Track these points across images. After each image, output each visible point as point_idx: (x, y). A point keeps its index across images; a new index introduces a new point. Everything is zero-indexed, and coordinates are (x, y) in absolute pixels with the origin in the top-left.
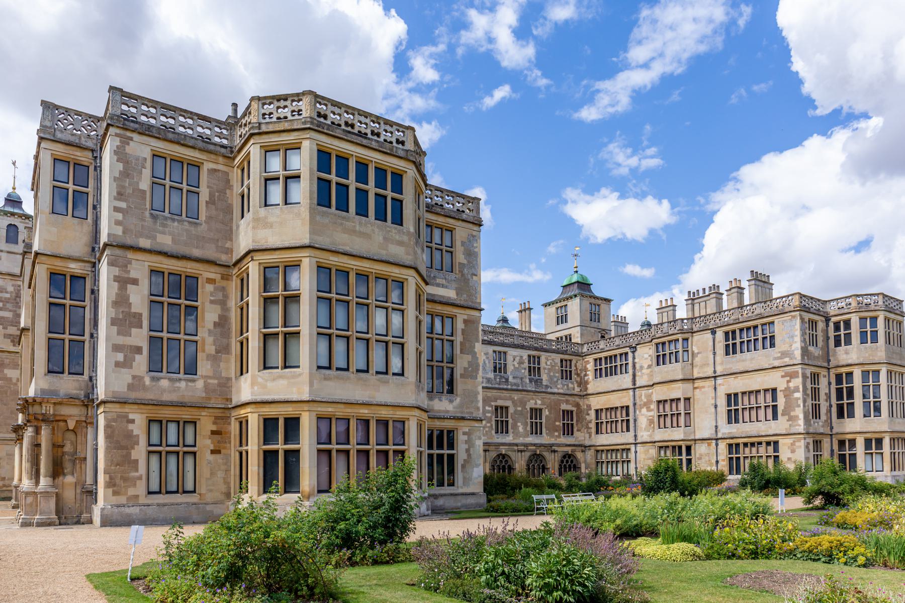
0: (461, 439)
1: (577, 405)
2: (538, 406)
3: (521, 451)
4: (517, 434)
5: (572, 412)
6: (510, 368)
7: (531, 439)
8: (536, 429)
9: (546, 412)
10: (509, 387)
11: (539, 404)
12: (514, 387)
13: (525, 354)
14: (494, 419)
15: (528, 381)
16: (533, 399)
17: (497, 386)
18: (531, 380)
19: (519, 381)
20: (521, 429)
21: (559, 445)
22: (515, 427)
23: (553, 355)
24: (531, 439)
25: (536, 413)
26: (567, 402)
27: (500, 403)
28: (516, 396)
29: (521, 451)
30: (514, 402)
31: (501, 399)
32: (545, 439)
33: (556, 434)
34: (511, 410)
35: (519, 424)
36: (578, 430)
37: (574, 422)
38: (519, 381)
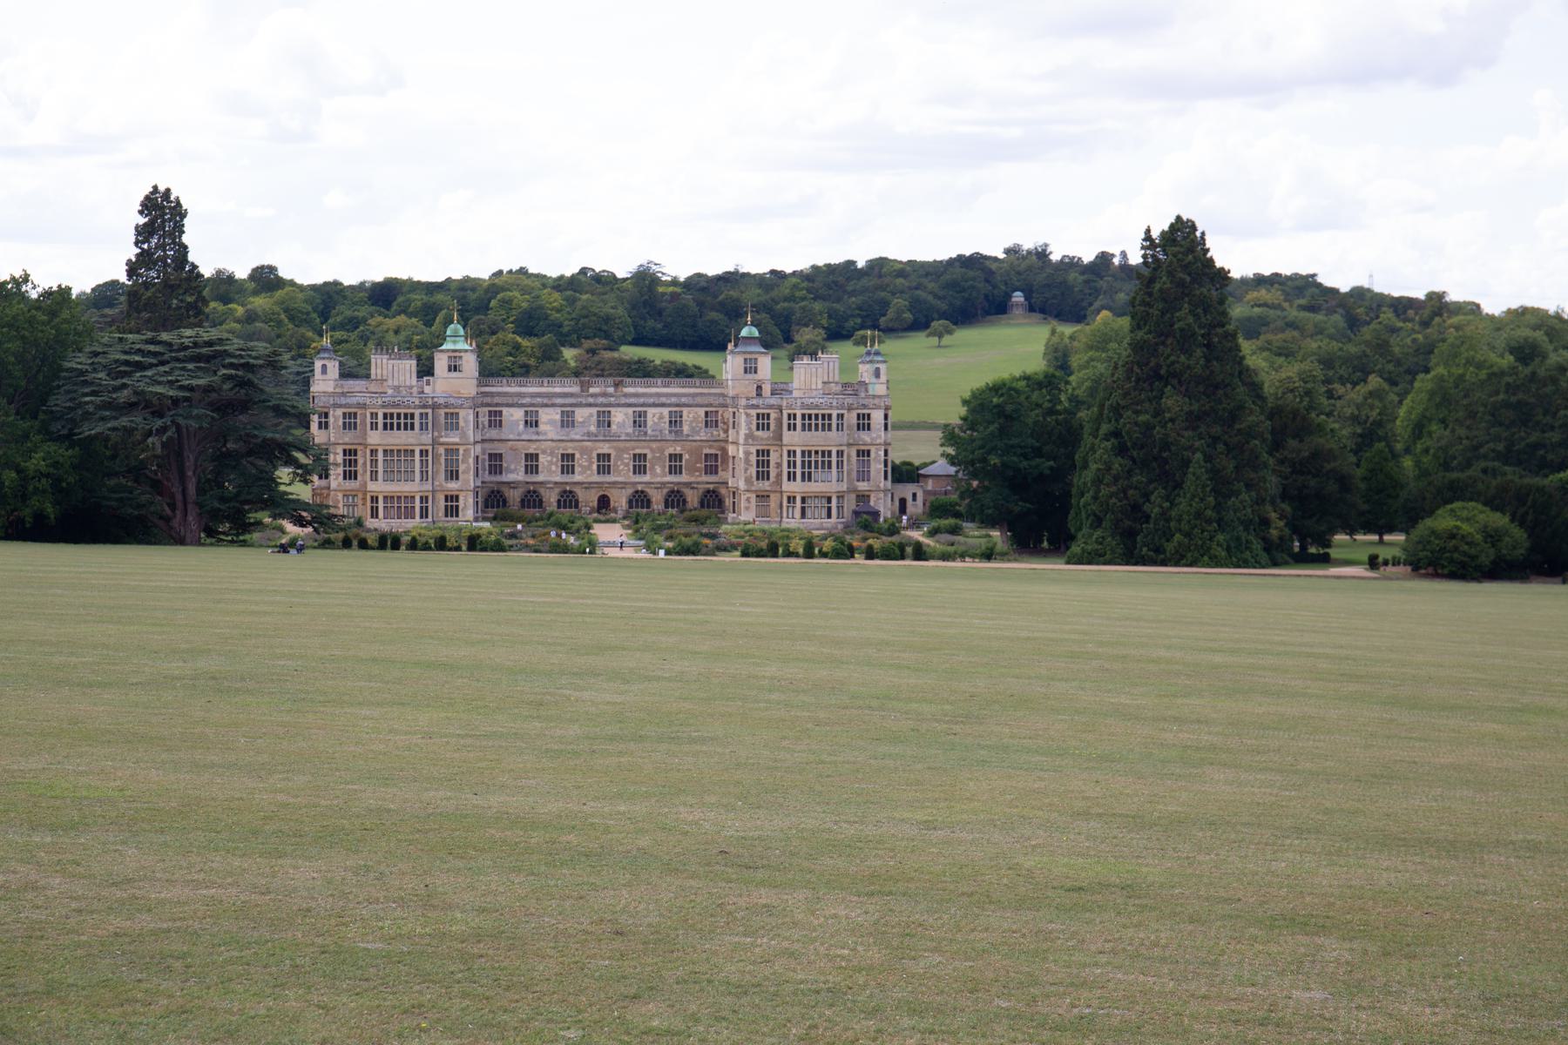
0: (461, 499)
1: (725, 451)
4: (654, 474)
6: (650, 423)
7: (669, 478)
8: (675, 470)
9: (686, 457)
11: (678, 450)
13: (665, 411)
22: (653, 468)
24: (669, 478)
25: (675, 457)
27: (638, 451)
28: (654, 445)
30: (652, 450)
32: (684, 478)
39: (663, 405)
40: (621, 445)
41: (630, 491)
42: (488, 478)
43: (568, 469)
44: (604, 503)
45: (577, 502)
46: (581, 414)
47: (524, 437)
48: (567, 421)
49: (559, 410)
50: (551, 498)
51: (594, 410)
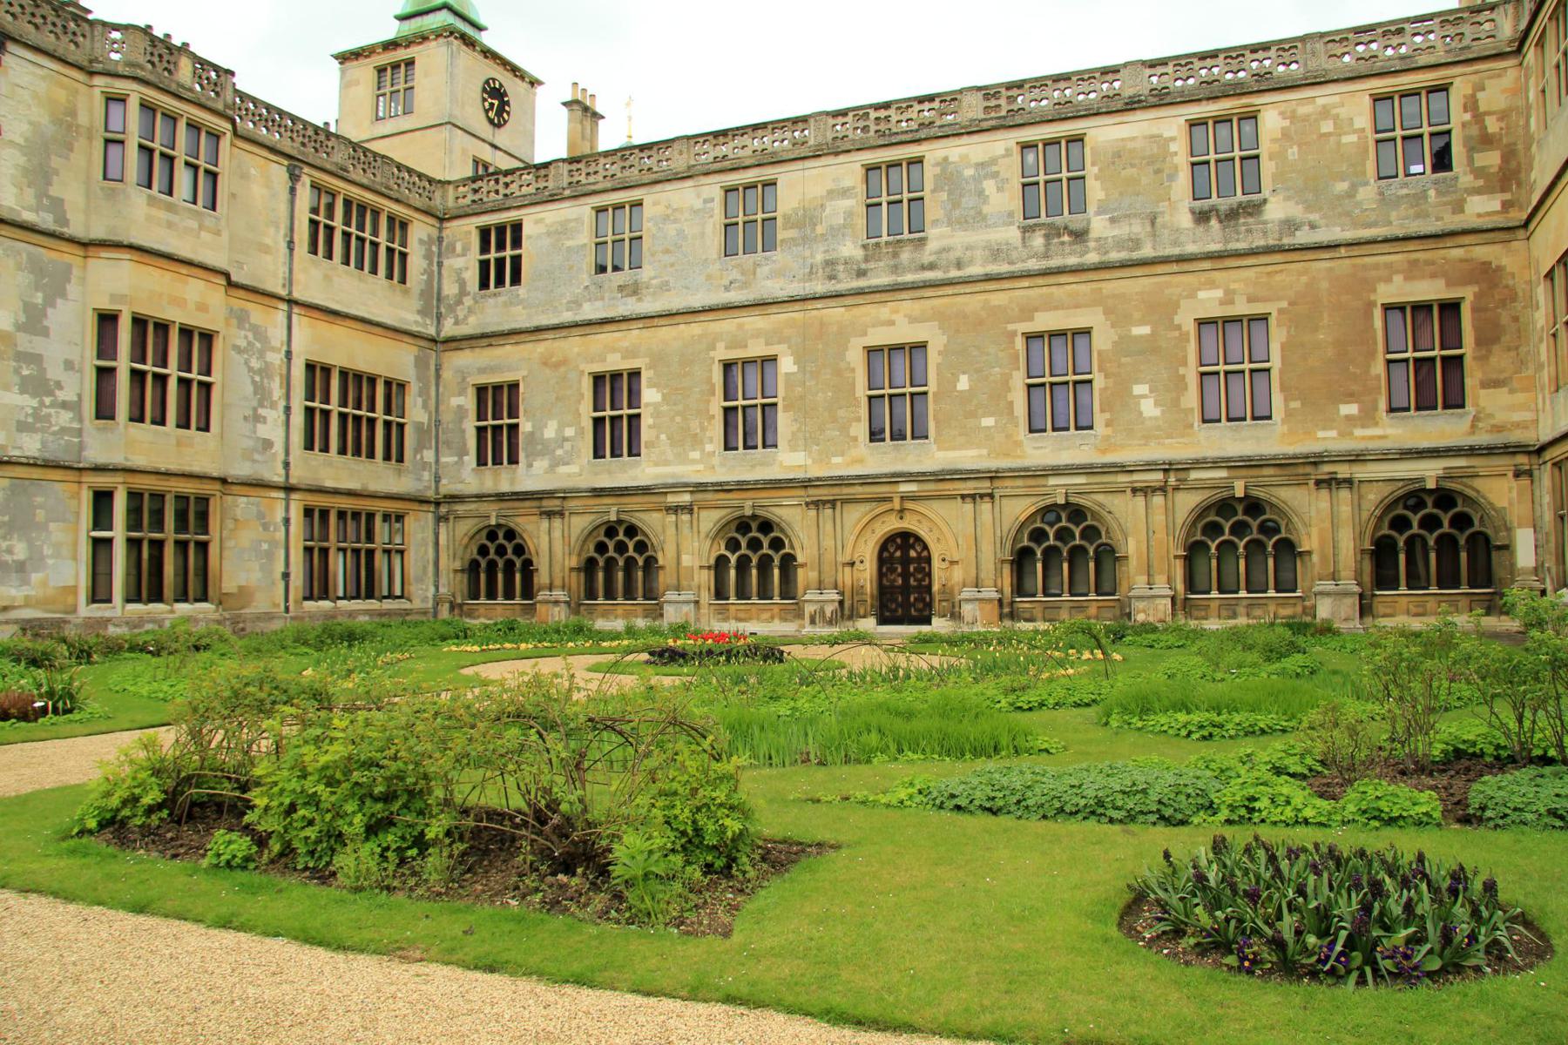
2: (1241, 308)
3: (1146, 491)
5: (1451, 308)
10: (1092, 258)
12: (1114, 256)
13: (1171, 125)
14: (1019, 380)
15: (1185, 220)
16: (1212, 285)
17: (1033, 265)
18: (1202, 217)
19: (1138, 228)
20: (1149, 408)
21: (1357, 458)
22: (1121, 397)
23: (1324, 96)
26: (1412, 272)
27: (1046, 321)
29: (1146, 491)
30: (1118, 315)
31: (1051, 306)
33: (1350, 409)
34: (1102, 340)
35: (1140, 389)
36: (1485, 385)
37: (1468, 348)
38: (1138, 228)
39: (1162, 99)
40: (971, 302)
41: (1018, 508)
42: (467, 476)
43: (746, 425)
44: (904, 584)
45: (788, 562)
46: (797, 187)
47: (590, 311)
48: (750, 228)
49: (712, 188)
50: (687, 549)
51: (848, 171)
